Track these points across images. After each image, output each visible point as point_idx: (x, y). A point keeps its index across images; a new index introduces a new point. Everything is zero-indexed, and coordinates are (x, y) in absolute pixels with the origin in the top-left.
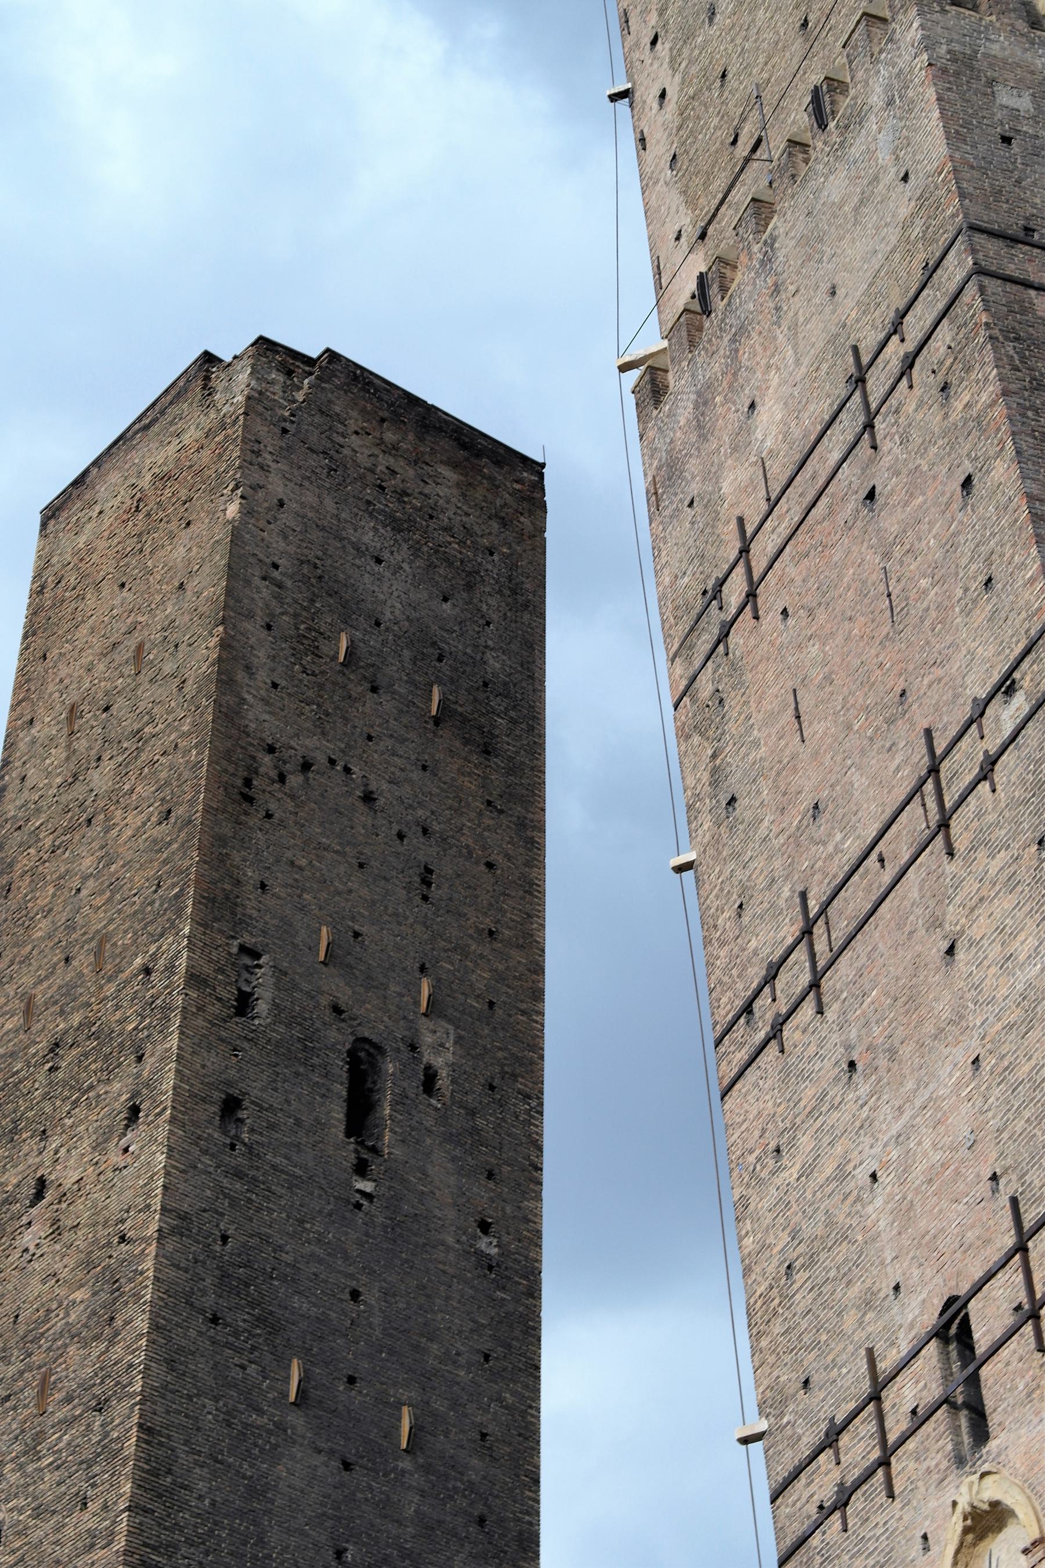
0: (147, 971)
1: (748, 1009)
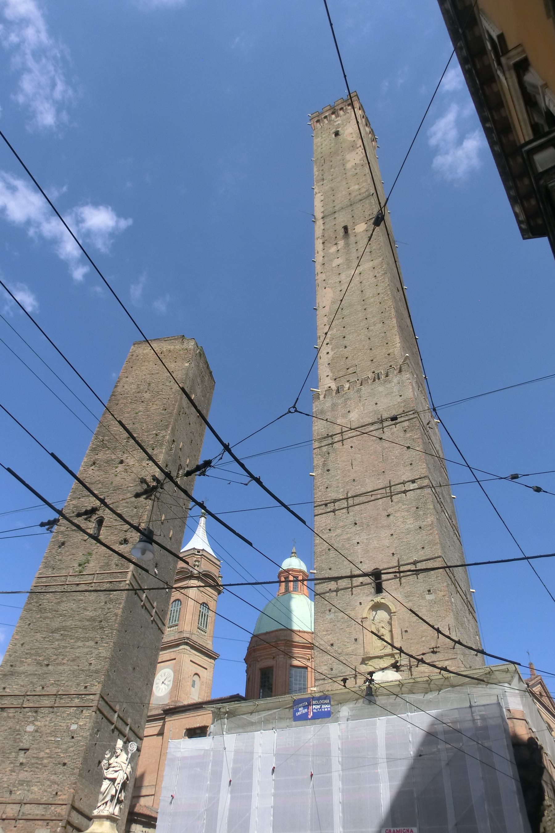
0: (157, 435)
1: (326, 505)
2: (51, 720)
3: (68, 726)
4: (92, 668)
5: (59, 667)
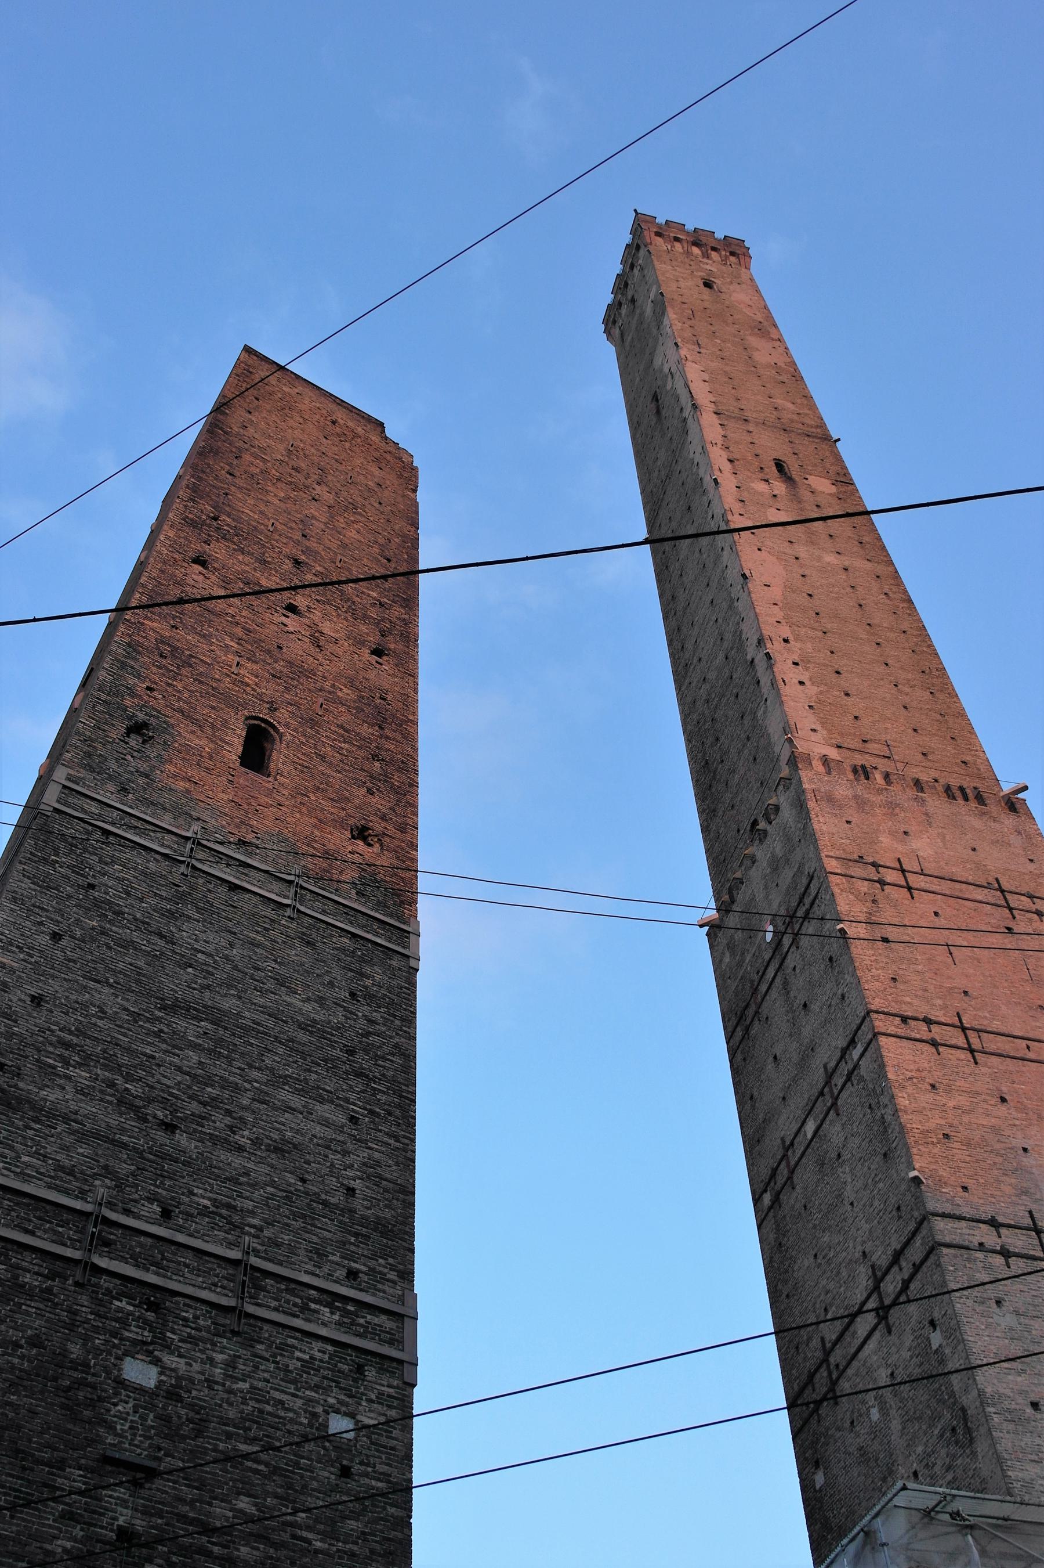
2: (231, 1364)
3: (315, 1415)
4: (358, 1203)
5: (224, 1156)
